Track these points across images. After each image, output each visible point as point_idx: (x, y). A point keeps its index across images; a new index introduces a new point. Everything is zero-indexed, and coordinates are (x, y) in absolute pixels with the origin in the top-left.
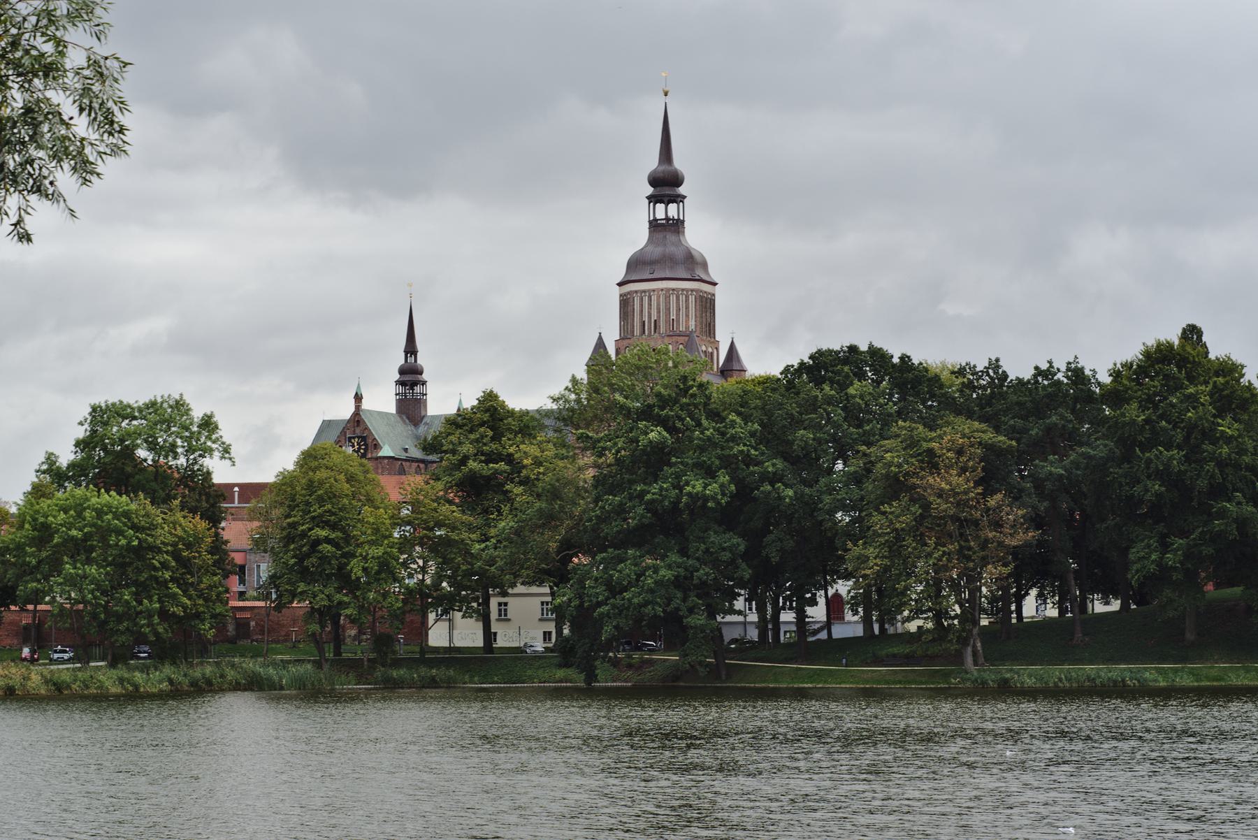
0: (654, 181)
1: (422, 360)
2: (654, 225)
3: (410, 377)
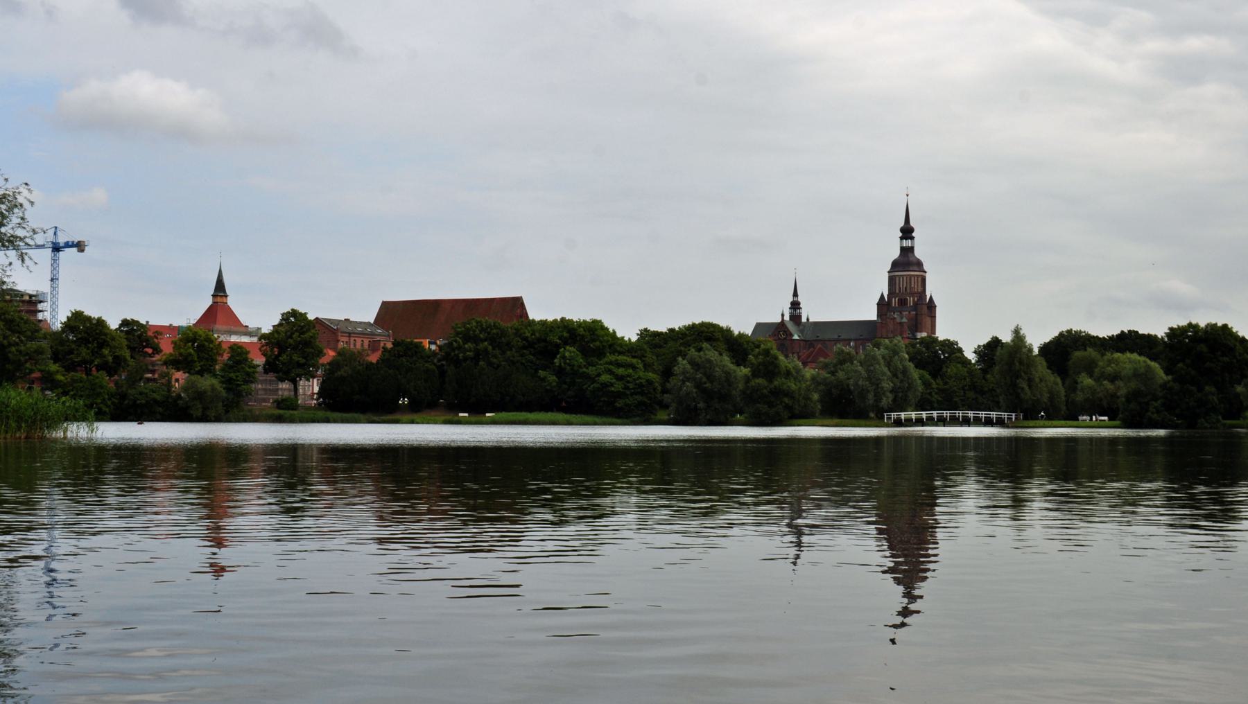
0: (902, 230)
1: (800, 299)
2: (902, 249)
3: (795, 305)
